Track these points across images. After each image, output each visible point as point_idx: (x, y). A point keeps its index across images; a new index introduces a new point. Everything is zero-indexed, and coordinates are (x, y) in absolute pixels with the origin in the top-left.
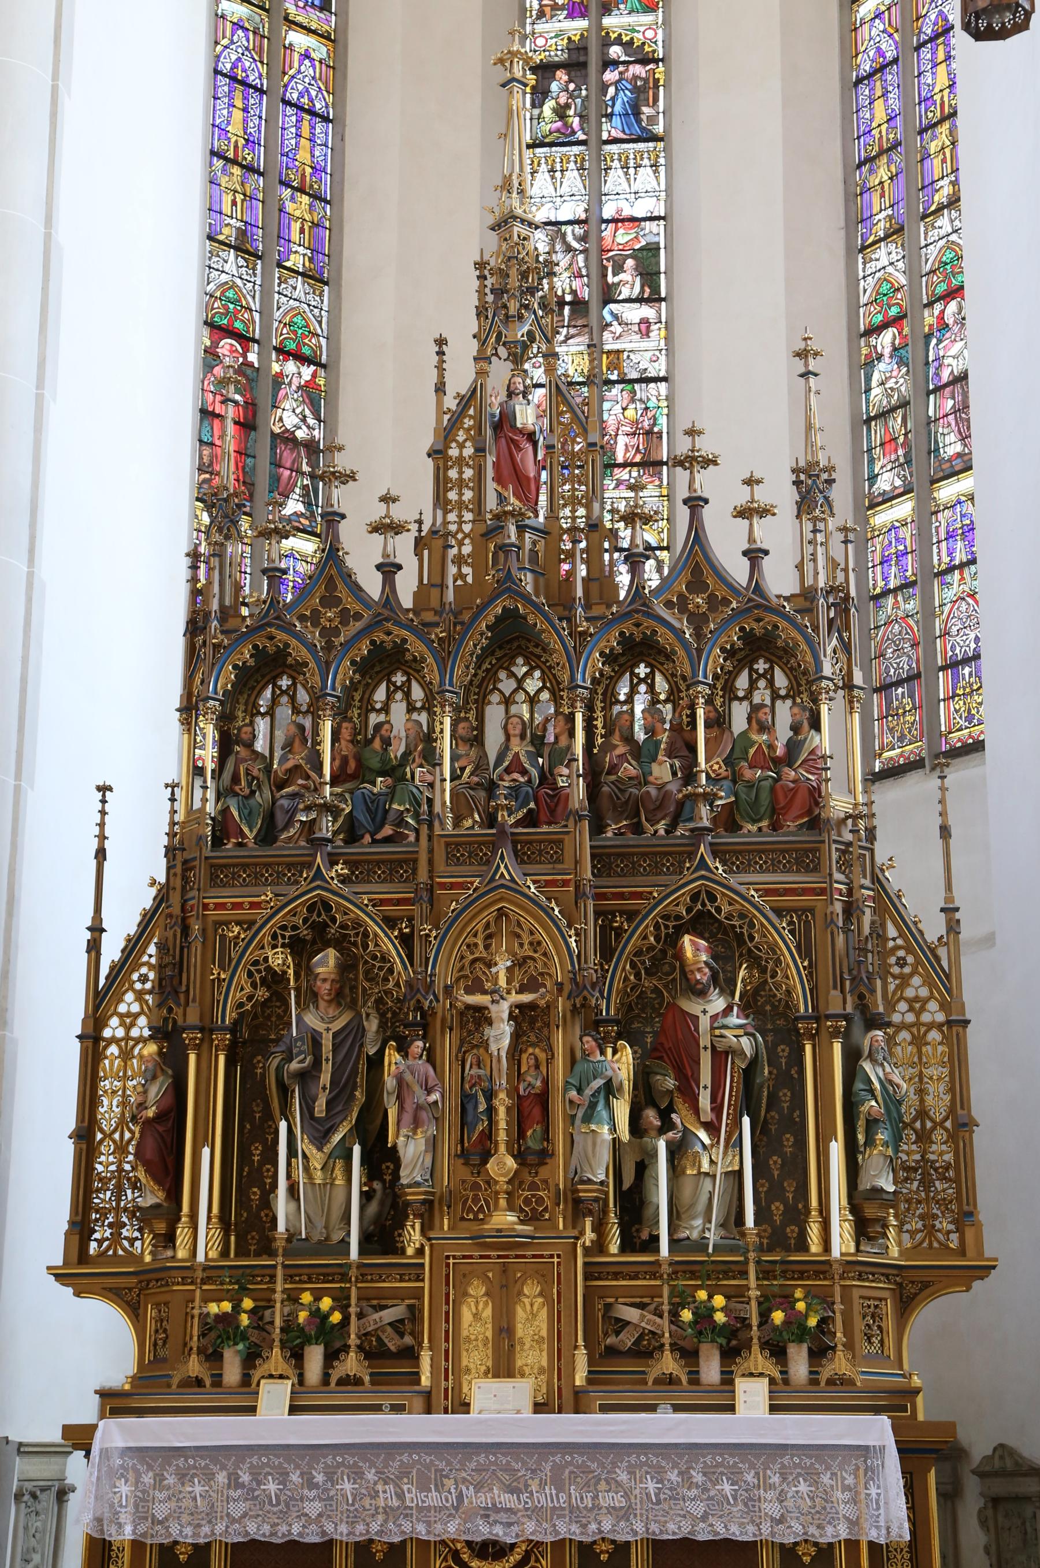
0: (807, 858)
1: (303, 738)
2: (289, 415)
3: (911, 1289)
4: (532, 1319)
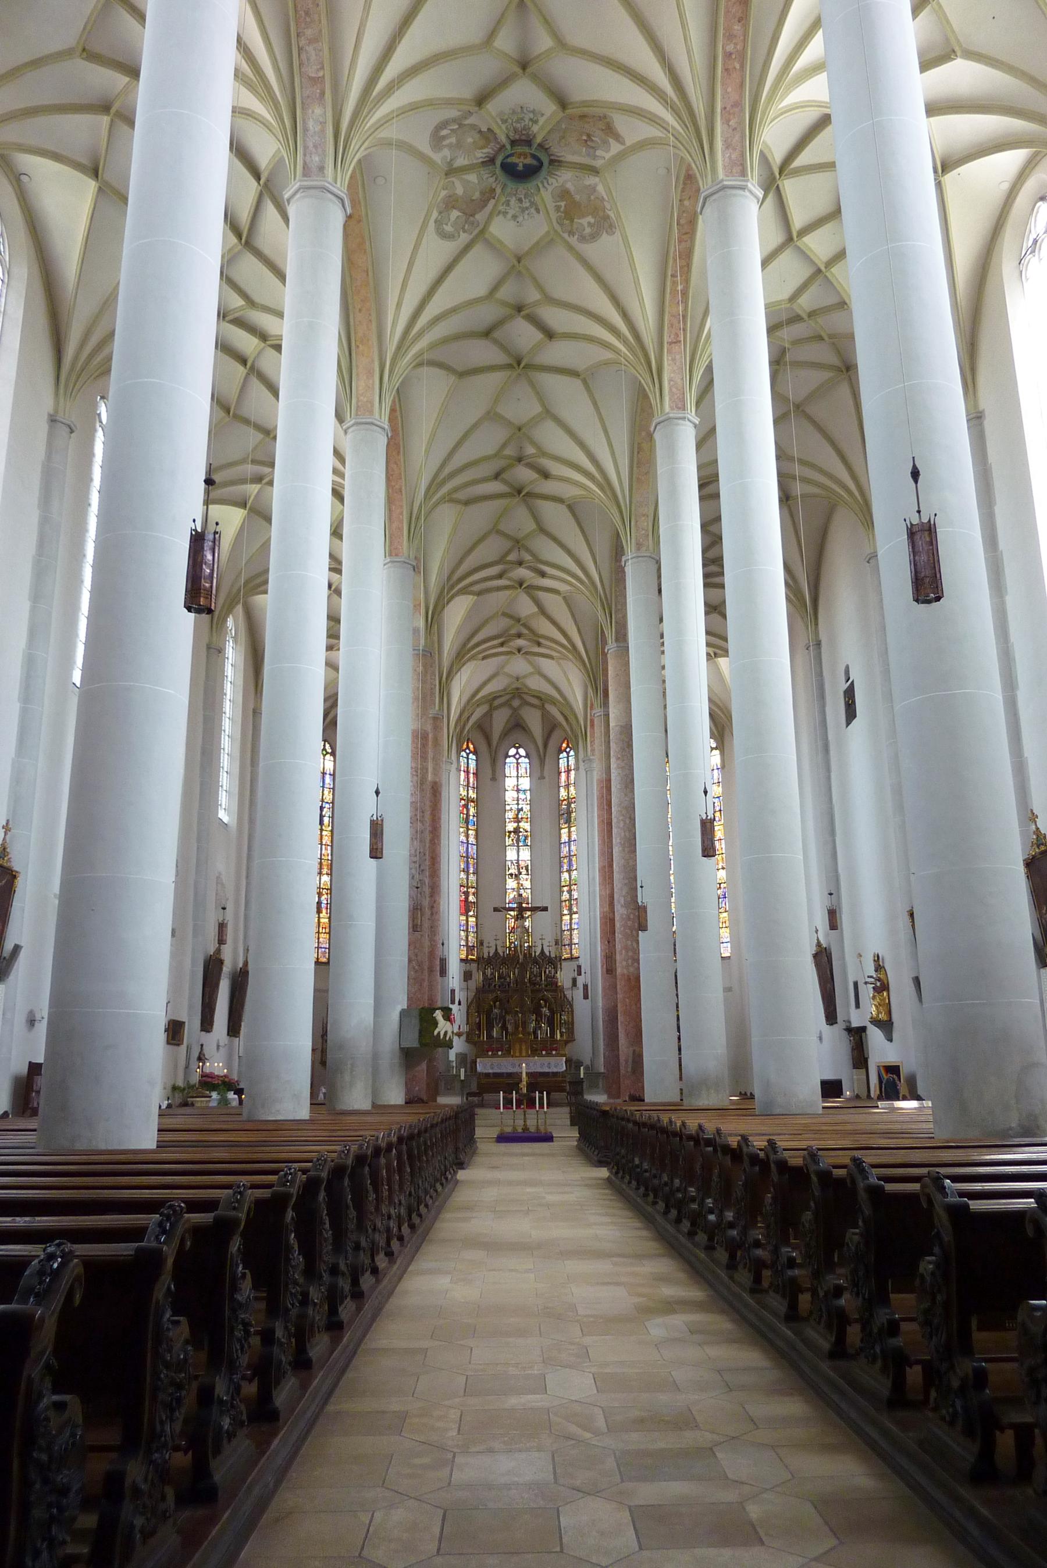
0: (555, 991)
1: (492, 974)
2: (471, 898)
3: (566, 1042)
4: (524, 1047)
